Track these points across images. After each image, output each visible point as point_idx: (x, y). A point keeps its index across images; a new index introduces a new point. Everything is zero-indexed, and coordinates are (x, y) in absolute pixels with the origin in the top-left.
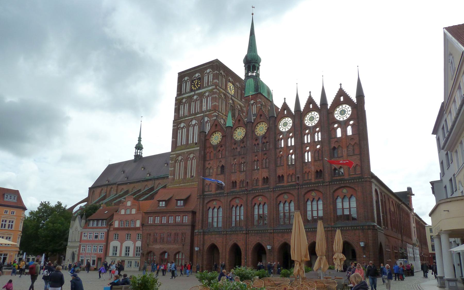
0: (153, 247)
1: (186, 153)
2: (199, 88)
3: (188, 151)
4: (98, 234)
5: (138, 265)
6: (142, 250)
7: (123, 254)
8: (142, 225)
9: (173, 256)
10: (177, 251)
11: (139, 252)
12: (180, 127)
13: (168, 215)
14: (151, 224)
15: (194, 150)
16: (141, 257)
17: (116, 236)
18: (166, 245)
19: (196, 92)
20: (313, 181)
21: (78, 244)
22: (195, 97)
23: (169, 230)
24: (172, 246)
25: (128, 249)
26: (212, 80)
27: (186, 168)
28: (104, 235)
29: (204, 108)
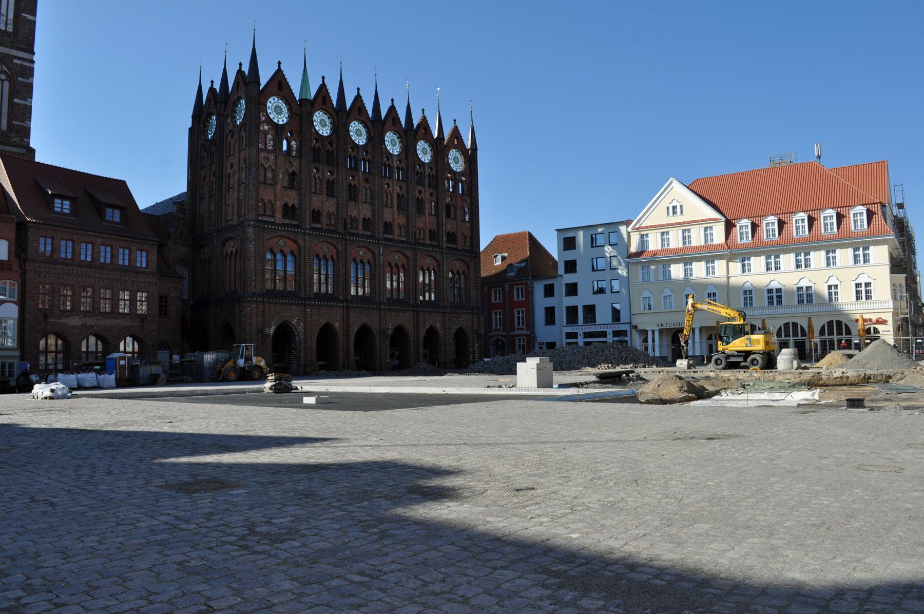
20: (428, 242)
23: (106, 281)
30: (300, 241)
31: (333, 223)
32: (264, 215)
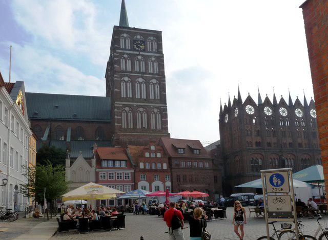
2: (144, 50)
17: (142, 177)
19: (141, 53)
22: (140, 57)
26: (156, 48)
27: (135, 119)
29: (151, 70)
30: (263, 154)
31: (276, 146)
32: (248, 146)
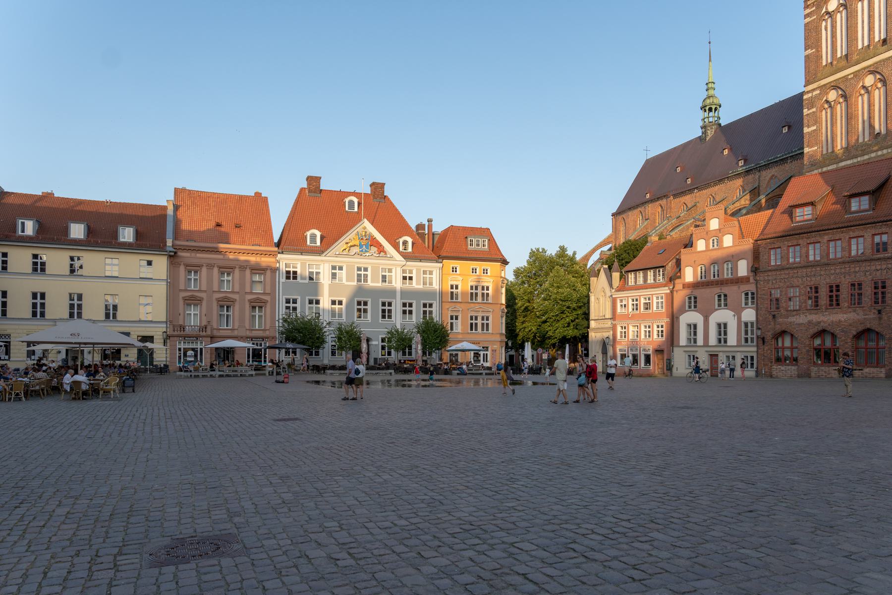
0: (789, 320)
1: (852, 76)
3: (859, 71)
4: (649, 299)
5: (752, 364)
6: (758, 328)
7: (713, 341)
8: (755, 270)
9: (849, 340)
10: (861, 328)
11: (752, 333)
12: (827, 13)
13: (826, 238)
14: (779, 265)
15: (876, 63)
16: (757, 346)
18: (827, 313)
21: (609, 324)
24: (845, 315)
25: (722, 329)
28: (663, 300)
